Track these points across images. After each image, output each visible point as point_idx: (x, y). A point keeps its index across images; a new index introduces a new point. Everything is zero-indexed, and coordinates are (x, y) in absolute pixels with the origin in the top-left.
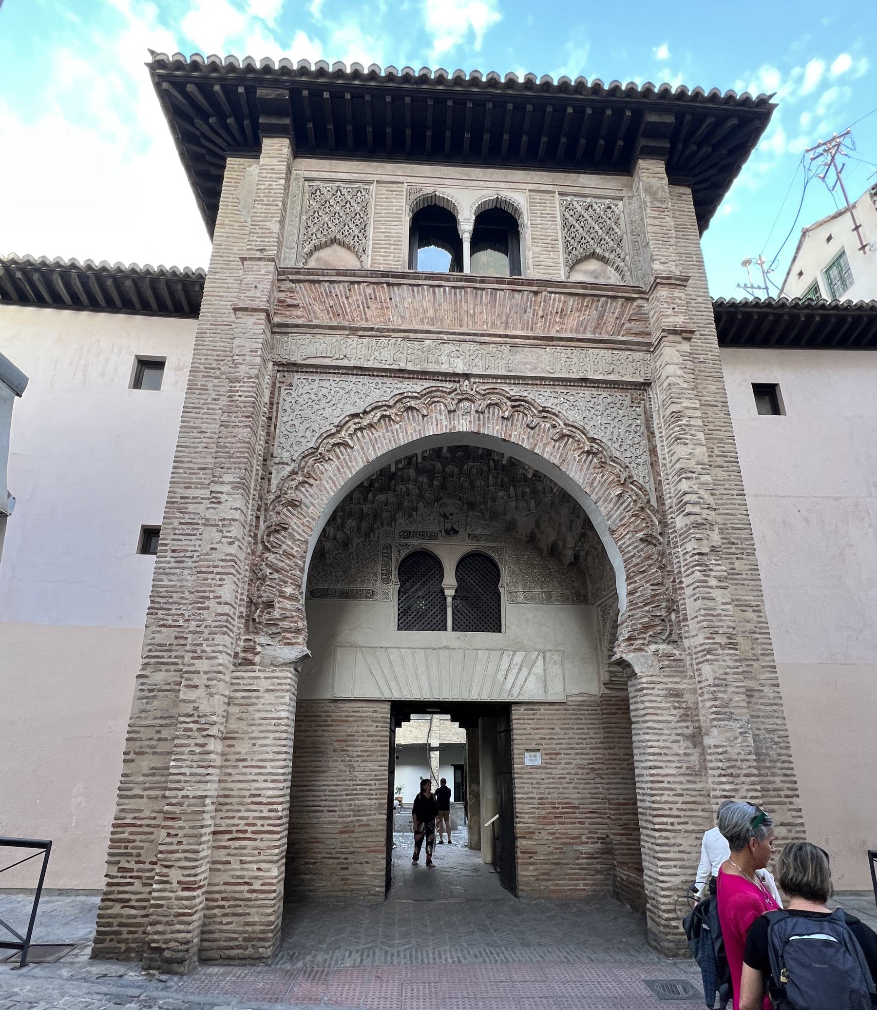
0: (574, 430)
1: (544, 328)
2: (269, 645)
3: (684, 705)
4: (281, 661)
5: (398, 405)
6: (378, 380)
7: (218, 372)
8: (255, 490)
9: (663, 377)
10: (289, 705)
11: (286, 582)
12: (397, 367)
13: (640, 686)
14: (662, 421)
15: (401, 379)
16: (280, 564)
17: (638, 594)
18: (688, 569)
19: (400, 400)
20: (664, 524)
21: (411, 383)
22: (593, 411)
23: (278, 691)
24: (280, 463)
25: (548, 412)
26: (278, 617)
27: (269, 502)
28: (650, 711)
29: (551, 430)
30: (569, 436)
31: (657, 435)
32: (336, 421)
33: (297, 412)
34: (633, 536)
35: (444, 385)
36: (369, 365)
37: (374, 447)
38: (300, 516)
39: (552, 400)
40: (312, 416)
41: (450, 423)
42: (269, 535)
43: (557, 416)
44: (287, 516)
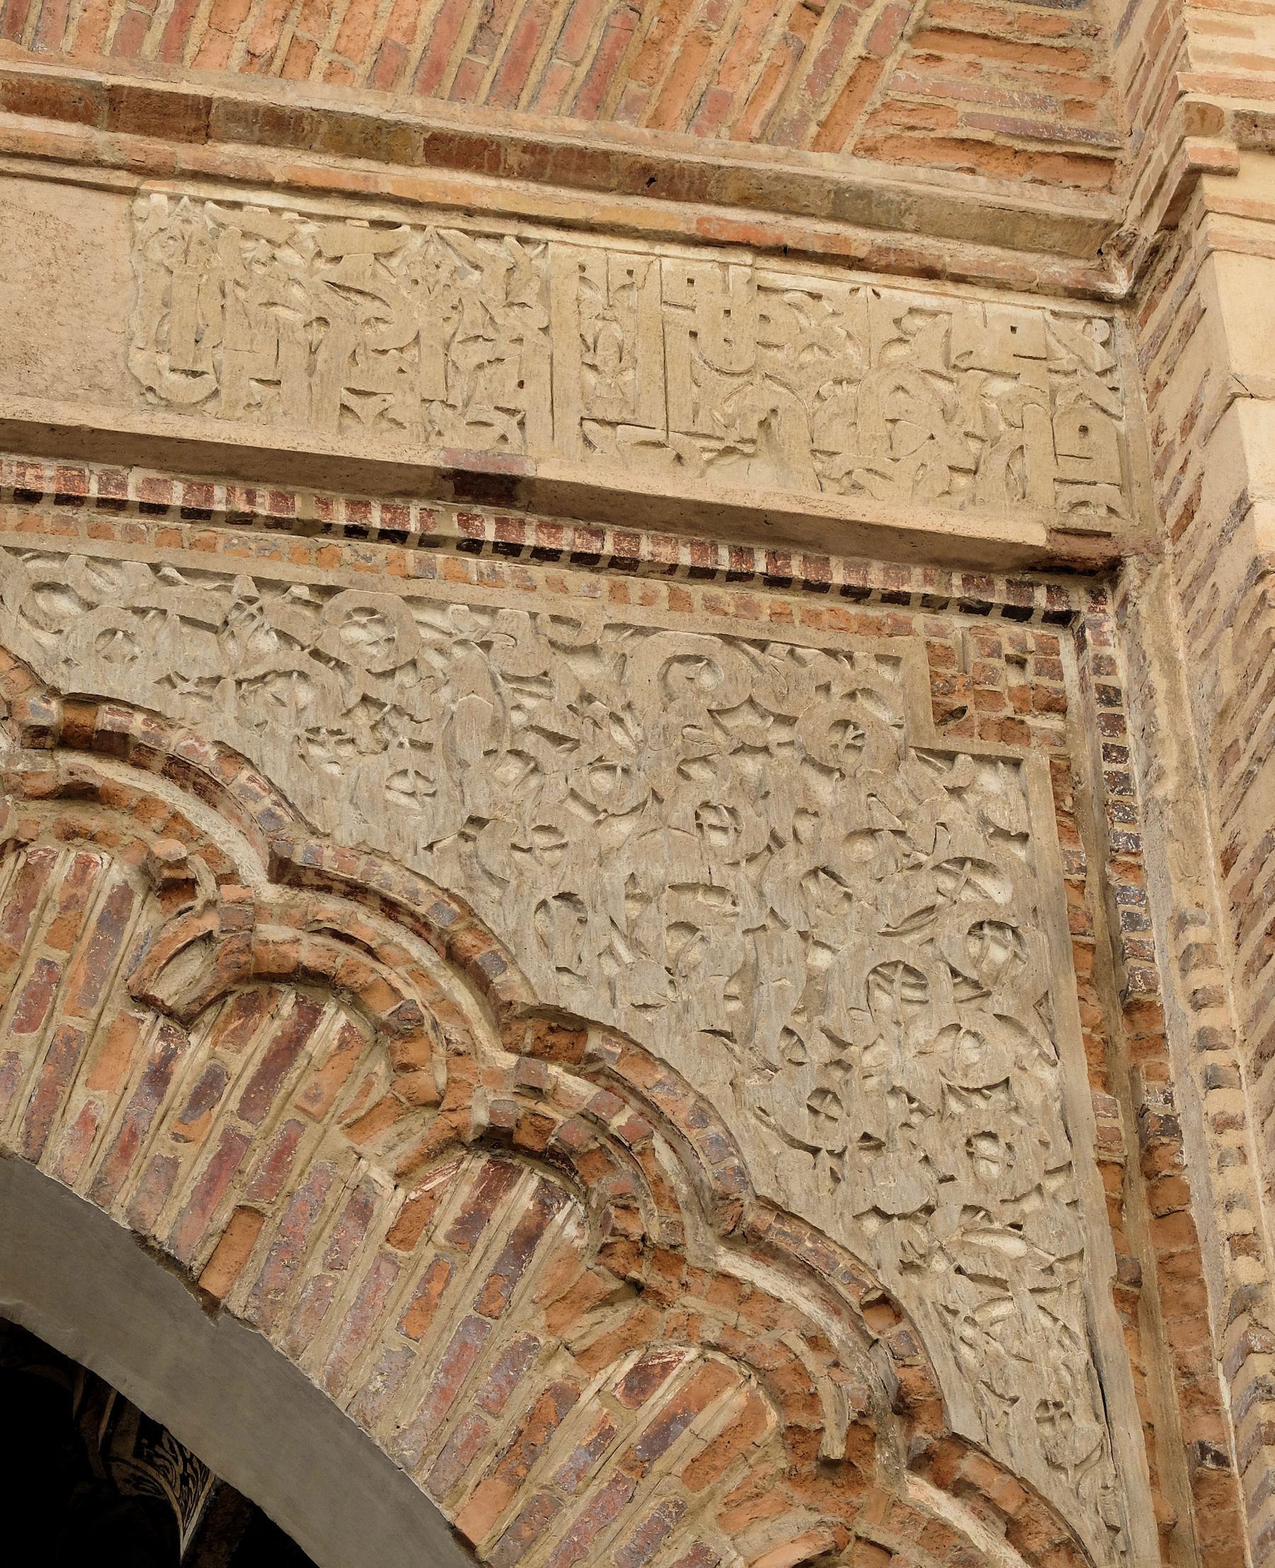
1: (135, 27)
14: (1217, 896)
25: (113, 745)
31: (1181, 1021)
43: (206, 788)
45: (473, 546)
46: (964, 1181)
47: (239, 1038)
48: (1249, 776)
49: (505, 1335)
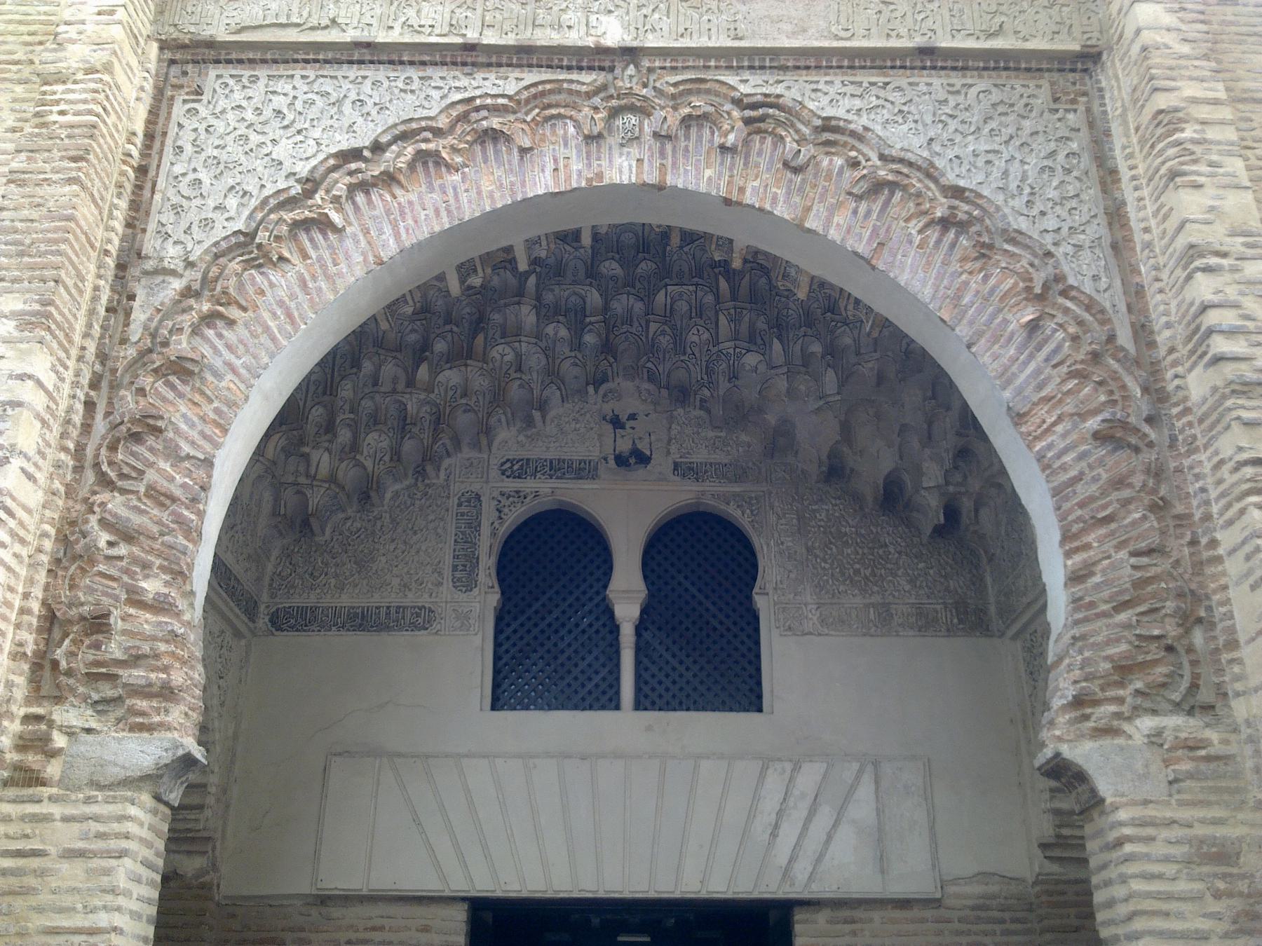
0: (905, 170)
2: (89, 731)
3: (1243, 886)
4: (115, 773)
5: (458, 130)
6: (413, 73)
7: (26, 71)
8: (86, 335)
9: (1129, 33)
10: (127, 894)
11: (146, 566)
12: (459, 40)
13: (1112, 836)
14: (1135, 140)
15: (467, 69)
16: (137, 520)
17: (1097, 579)
18: (1229, 506)
19: (464, 117)
20: (1157, 393)
21: (492, 76)
22: (953, 124)
23: (95, 854)
24: (156, 272)
25: (836, 130)
26: (118, 655)
27: (121, 366)
28: (1148, 905)
29: (847, 173)
30: (893, 186)
31: (1125, 174)
32: (303, 169)
33: (211, 151)
34: (1075, 426)
35: (574, 76)
36: (394, 36)
37: (395, 227)
38: (197, 398)
39: (847, 103)
40: (243, 159)
41: (589, 165)
42: (113, 448)
43: (860, 138)
44: (164, 399)
45: (924, 68)
46: (1069, 221)
47: (874, 201)
48: (1143, 106)
49: (951, 269)
